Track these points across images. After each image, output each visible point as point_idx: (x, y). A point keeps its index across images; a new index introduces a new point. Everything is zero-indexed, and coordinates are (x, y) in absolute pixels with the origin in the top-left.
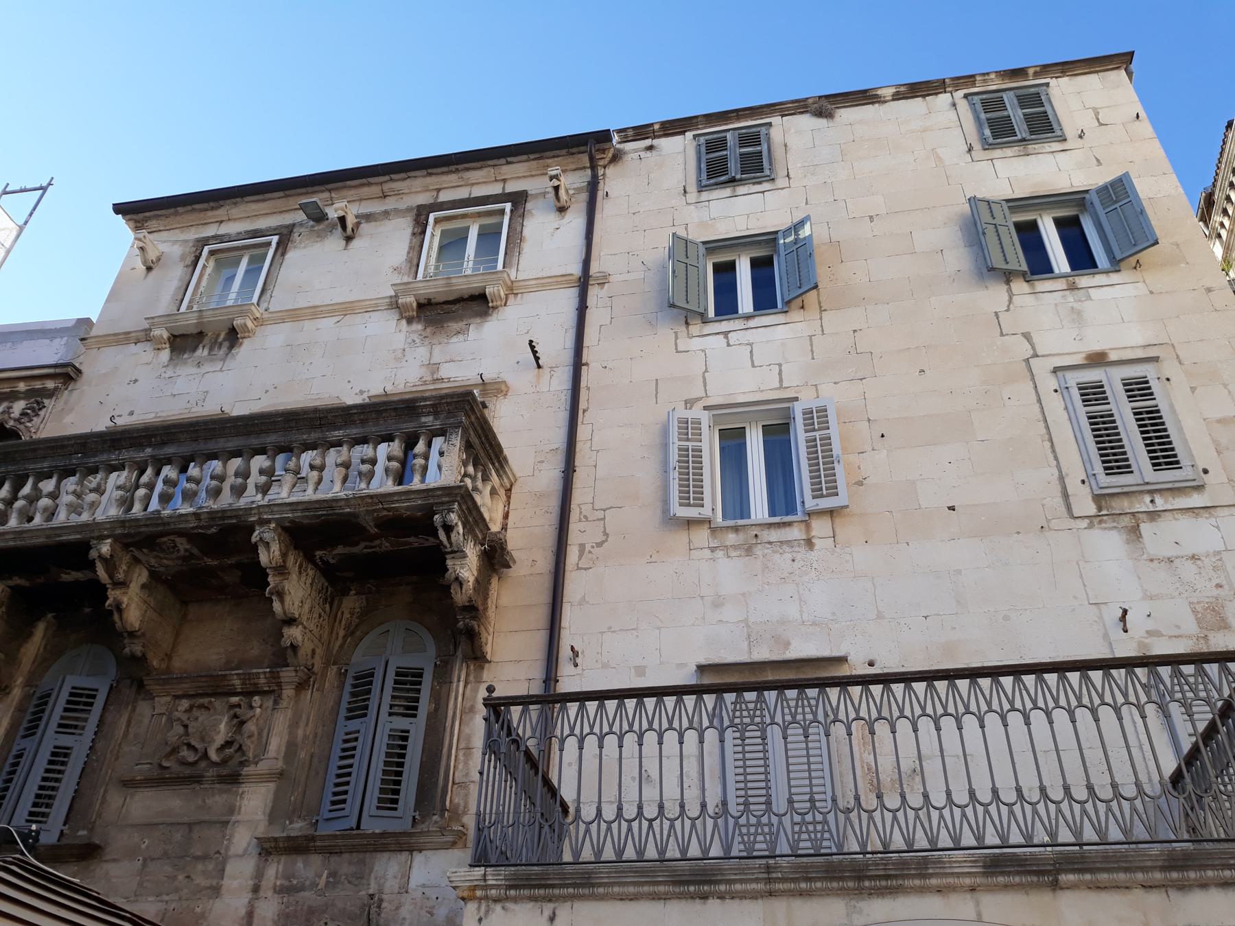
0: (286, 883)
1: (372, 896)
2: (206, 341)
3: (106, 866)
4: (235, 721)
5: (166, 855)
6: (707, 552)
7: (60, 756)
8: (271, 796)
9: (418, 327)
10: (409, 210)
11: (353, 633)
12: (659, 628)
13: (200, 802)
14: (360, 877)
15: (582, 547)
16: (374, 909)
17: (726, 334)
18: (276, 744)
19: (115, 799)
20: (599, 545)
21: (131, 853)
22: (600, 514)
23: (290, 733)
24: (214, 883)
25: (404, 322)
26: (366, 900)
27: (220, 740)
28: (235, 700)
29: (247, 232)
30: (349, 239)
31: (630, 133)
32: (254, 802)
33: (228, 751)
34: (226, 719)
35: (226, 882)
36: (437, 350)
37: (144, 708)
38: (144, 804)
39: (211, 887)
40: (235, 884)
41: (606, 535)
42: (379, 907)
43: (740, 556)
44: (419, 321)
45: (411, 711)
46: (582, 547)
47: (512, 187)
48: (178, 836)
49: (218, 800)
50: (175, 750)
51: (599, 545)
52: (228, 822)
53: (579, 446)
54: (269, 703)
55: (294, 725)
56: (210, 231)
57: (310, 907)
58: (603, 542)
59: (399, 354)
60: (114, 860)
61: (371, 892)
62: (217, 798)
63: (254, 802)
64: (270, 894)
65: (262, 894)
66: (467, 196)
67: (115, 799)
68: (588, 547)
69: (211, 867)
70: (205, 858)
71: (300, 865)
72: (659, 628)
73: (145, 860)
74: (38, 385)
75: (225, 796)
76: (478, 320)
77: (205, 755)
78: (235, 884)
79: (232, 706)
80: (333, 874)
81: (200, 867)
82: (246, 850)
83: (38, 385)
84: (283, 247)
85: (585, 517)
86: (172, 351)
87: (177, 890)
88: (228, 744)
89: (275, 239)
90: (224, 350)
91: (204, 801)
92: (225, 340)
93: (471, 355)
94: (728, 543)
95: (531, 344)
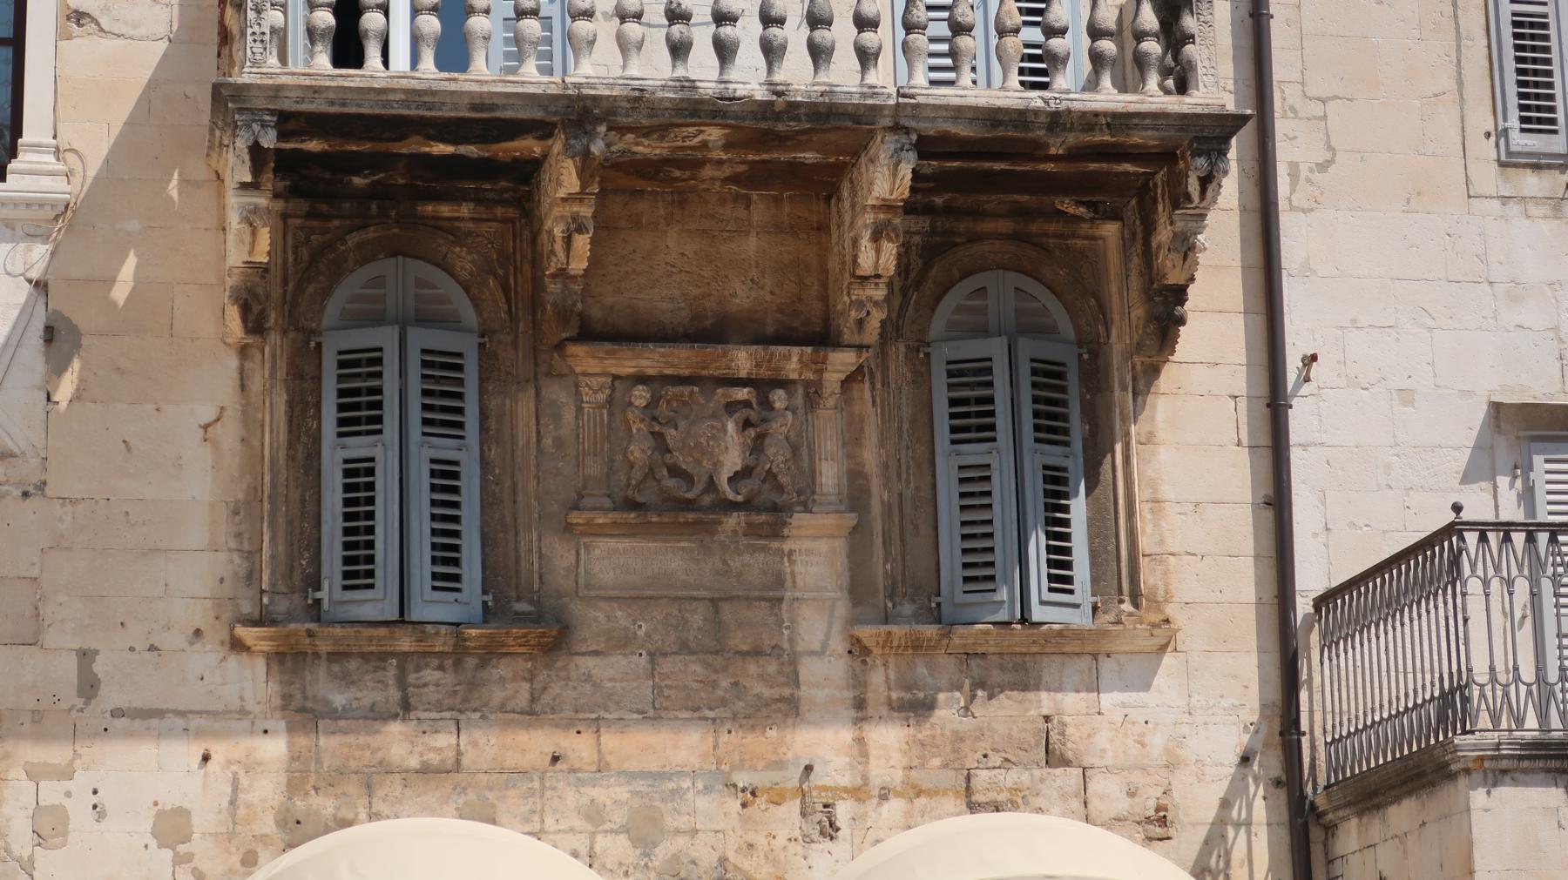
0: (908, 696)
1: (1047, 719)
3: (588, 664)
4: (752, 432)
5: (684, 648)
6: (1496, 203)
8: (842, 563)
11: (918, 285)
12: (1430, 329)
13: (718, 564)
16: (1054, 737)
18: (830, 475)
19: (561, 554)
20: (1323, 167)
21: (623, 643)
23: (850, 456)
24: (787, 692)
26: (1042, 725)
27: (733, 460)
28: (742, 393)
34: (731, 426)
35: (804, 692)
37: (557, 393)
38: (614, 559)
39: (782, 700)
41: (1331, 148)
42: (1063, 734)
43: (1545, 217)
46: (1294, 168)
48: (697, 618)
49: (752, 564)
50: (651, 472)
51: (1323, 167)
52: (780, 600)
54: (799, 399)
55: (852, 439)
57: (955, 733)
58: (1330, 162)
60: (596, 653)
61: (1045, 712)
62: (747, 558)
64: (884, 711)
65: (870, 711)
67: (561, 554)
68: (1304, 169)
70: (757, 653)
71: (922, 670)
72: (1430, 329)
73: (651, 654)
75: (761, 557)
77: (711, 485)
78: (822, 695)
79: (731, 407)
81: (753, 668)
82: (825, 645)
85: (1292, 109)
87: (724, 703)
91: (725, 563)
94: (1527, 193)
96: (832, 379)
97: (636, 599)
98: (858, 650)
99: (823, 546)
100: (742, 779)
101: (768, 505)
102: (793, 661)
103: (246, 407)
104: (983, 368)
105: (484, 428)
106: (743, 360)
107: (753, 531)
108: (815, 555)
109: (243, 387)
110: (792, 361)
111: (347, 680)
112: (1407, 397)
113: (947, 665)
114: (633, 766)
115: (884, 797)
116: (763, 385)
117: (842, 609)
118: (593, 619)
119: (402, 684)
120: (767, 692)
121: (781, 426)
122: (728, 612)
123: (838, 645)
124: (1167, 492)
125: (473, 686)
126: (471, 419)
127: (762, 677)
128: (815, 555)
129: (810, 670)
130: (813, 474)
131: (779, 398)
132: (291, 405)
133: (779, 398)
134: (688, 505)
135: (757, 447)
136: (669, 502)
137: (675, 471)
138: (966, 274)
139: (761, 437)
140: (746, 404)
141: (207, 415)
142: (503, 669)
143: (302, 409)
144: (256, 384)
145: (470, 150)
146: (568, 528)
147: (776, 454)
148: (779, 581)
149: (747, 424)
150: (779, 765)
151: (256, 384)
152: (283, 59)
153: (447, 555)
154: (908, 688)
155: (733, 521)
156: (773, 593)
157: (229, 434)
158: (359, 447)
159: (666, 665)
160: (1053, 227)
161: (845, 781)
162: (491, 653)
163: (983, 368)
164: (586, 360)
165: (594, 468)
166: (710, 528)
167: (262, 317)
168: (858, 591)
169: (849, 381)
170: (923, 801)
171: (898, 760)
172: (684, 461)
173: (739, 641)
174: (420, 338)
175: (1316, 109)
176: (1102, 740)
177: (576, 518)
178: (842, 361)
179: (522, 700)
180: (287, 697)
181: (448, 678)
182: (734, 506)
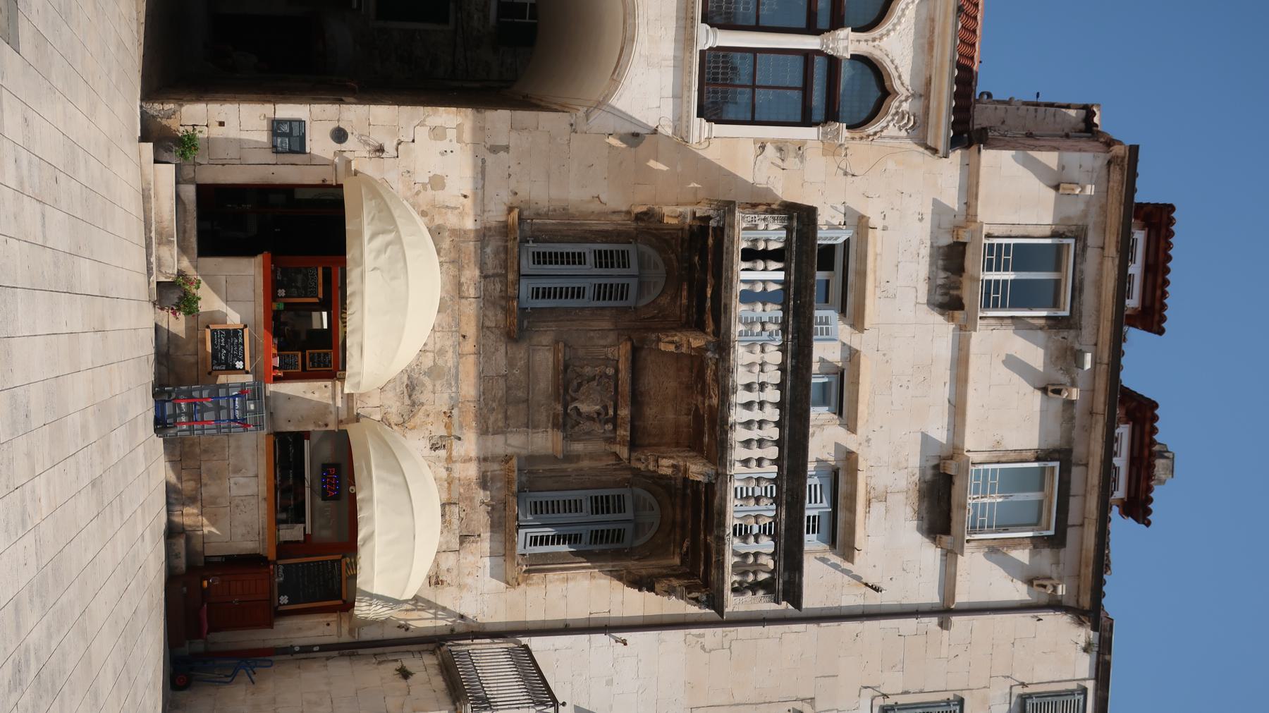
2: (954, 278)
3: (502, 349)
5: (508, 388)
8: (543, 452)
10: (1070, 440)
18: (578, 447)
19: (546, 339)
20: (703, 648)
21: (511, 364)
22: (726, 645)
25: (936, 462)
27: (584, 408)
28: (611, 412)
29: (1081, 282)
31: (1107, 635)
33: (573, 414)
35: (490, 437)
36: (902, 497)
37: (611, 338)
38: (545, 360)
40: (489, 444)
44: (934, 475)
46: (702, 636)
47: (1072, 534)
48: (520, 394)
49: (542, 416)
50: (579, 375)
51: (703, 648)
54: (608, 435)
55: (592, 456)
56: (1093, 239)
59: (905, 465)
66: (1072, 492)
67: (546, 339)
68: (701, 640)
69: (500, 424)
70: (506, 418)
71: (499, 485)
76: (925, 526)
77: (574, 400)
79: (605, 408)
81: (500, 416)
86: (949, 246)
87: (486, 404)
90: (939, 299)
92: (951, 296)
96: (617, 448)
97: (528, 369)
98: (507, 459)
99: (550, 444)
100: (455, 412)
101: (566, 423)
102: (503, 433)
103: (605, 214)
104: (621, 509)
105: (597, 308)
106: (624, 412)
107: (556, 416)
108: (545, 441)
109: (614, 212)
110: (624, 432)
111: (496, 253)
112: (610, 682)
113: (501, 495)
114: (461, 367)
115: (447, 469)
116: (614, 421)
117: (524, 452)
118: (520, 352)
119: (494, 275)
120: (490, 422)
121: (598, 428)
122: (523, 406)
123: (510, 451)
124: (571, 584)
125: (494, 304)
126: (601, 303)
127: (496, 420)
128: (545, 441)
129: (500, 439)
130: (578, 440)
131: (609, 427)
132: (607, 231)
133: (609, 427)
134: (566, 390)
135: (590, 418)
136: (567, 382)
137: (580, 385)
138: (659, 502)
139: (593, 419)
140: (607, 414)
141: (603, 198)
142: (500, 316)
143: (605, 236)
144: (615, 218)
145: (709, 304)
146: (557, 342)
147: (586, 426)
148: (535, 427)
149: (599, 414)
150: (461, 427)
151: (615, 218)
152: (745, 229)
153: (546, 293)
154: (492, 479)
155: (560, 408)
156: (530, 425)
157: (596, 207)
158: (590, 259)
159: (501, 382)
160: (678, 537)
161: (454, 453)
162: (507, 311)
163: (621, 509)
164: (624, 349)
165: (581, 352)
166: (557, 399)
167: (642, 220)
168: (531, 459)
169: (615, 454)
170: (446, 485)
171: (463, 475)
172: (583, 389)
173: (511, 411)
174: (633, 283)
175: (726, 645)
176: (470, 558)
177: (561, 345)
178: (624, 452)
179: (488, 323)
180: (490, 229)
181: (497, 293)
182: (565, 408)
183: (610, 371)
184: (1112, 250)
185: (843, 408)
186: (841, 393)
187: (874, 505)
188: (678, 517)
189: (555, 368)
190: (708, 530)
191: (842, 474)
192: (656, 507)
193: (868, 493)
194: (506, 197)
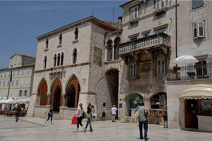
7: (135, 71)
9: (157, 16)
14: (162, 79)
15: (179, 44)
17: (195, 11)
21: (142, 78)
27: (147, 68)
30: (146, 4)
32: (151, 72)
45: (164, 64)
48: (146, 76)
51: (181, 44)
53: (177, 31)
63: (151, 72)
67: (140, 74)
74: (119, 31)
80: (159, 79)
83: (119, 31)
84: (139, 7)
88: (147, 68)
89: (138, 6)
93: (164, 21)
95: (170, 19)
96: (152, 63)
101: (148, 70)
106: (147, 62)
110: (149, 62)
116: (148, 64)
117: (152, 75)
118: (141, 77)
122: (147, 76)
129: (151, 79)
136: (144, 70)
148: (149, 74)
169: (153, 62)
172: (145, 68)
173: (147, 78)
183: (143, 65)
184: (131, 3)
185: (149, 32)
186: (146, 33)
187: (160, 23)
188: (161, 52)
189: (143, 72)
190: (155, 49)
191: (156, 29)
192: (159, 56)
193: (159, 25)
194: (126, 80)
